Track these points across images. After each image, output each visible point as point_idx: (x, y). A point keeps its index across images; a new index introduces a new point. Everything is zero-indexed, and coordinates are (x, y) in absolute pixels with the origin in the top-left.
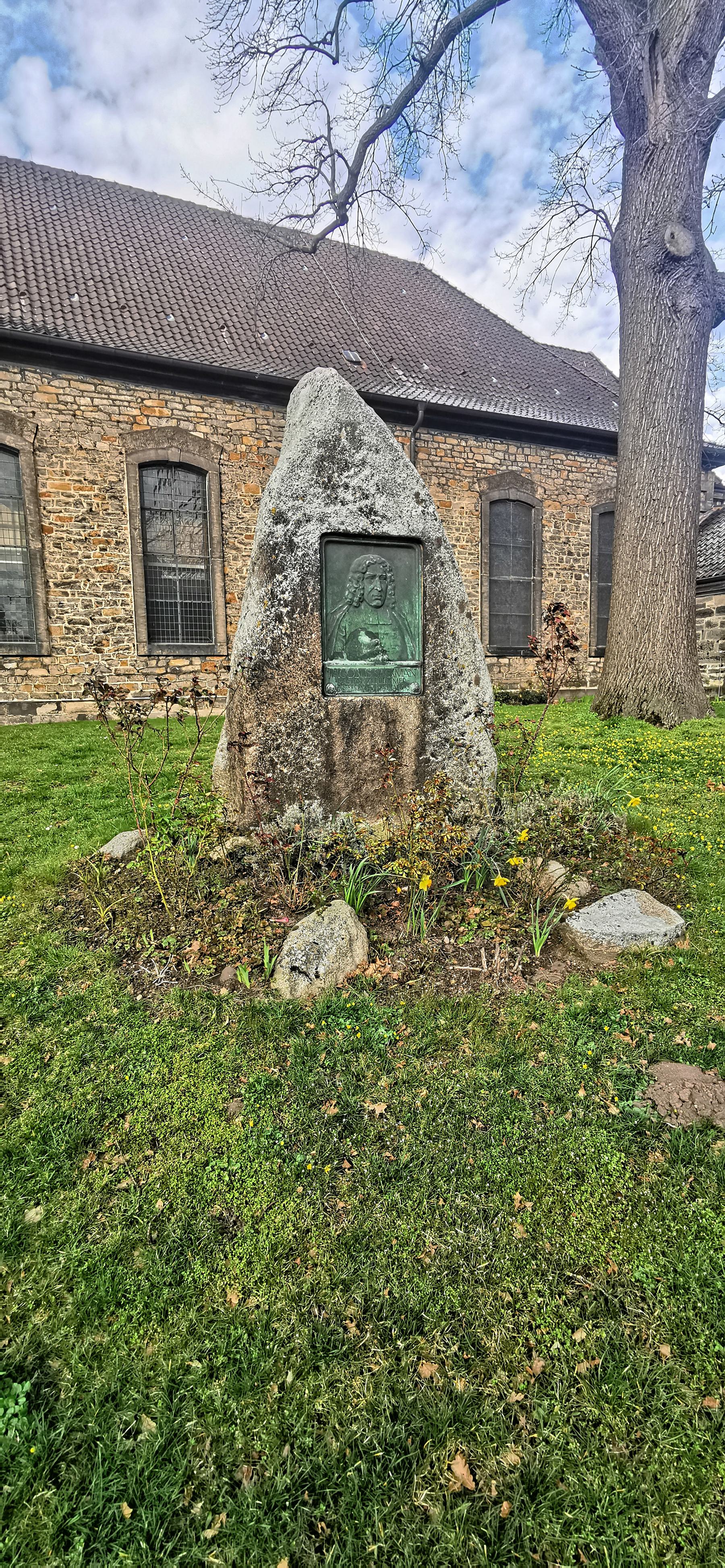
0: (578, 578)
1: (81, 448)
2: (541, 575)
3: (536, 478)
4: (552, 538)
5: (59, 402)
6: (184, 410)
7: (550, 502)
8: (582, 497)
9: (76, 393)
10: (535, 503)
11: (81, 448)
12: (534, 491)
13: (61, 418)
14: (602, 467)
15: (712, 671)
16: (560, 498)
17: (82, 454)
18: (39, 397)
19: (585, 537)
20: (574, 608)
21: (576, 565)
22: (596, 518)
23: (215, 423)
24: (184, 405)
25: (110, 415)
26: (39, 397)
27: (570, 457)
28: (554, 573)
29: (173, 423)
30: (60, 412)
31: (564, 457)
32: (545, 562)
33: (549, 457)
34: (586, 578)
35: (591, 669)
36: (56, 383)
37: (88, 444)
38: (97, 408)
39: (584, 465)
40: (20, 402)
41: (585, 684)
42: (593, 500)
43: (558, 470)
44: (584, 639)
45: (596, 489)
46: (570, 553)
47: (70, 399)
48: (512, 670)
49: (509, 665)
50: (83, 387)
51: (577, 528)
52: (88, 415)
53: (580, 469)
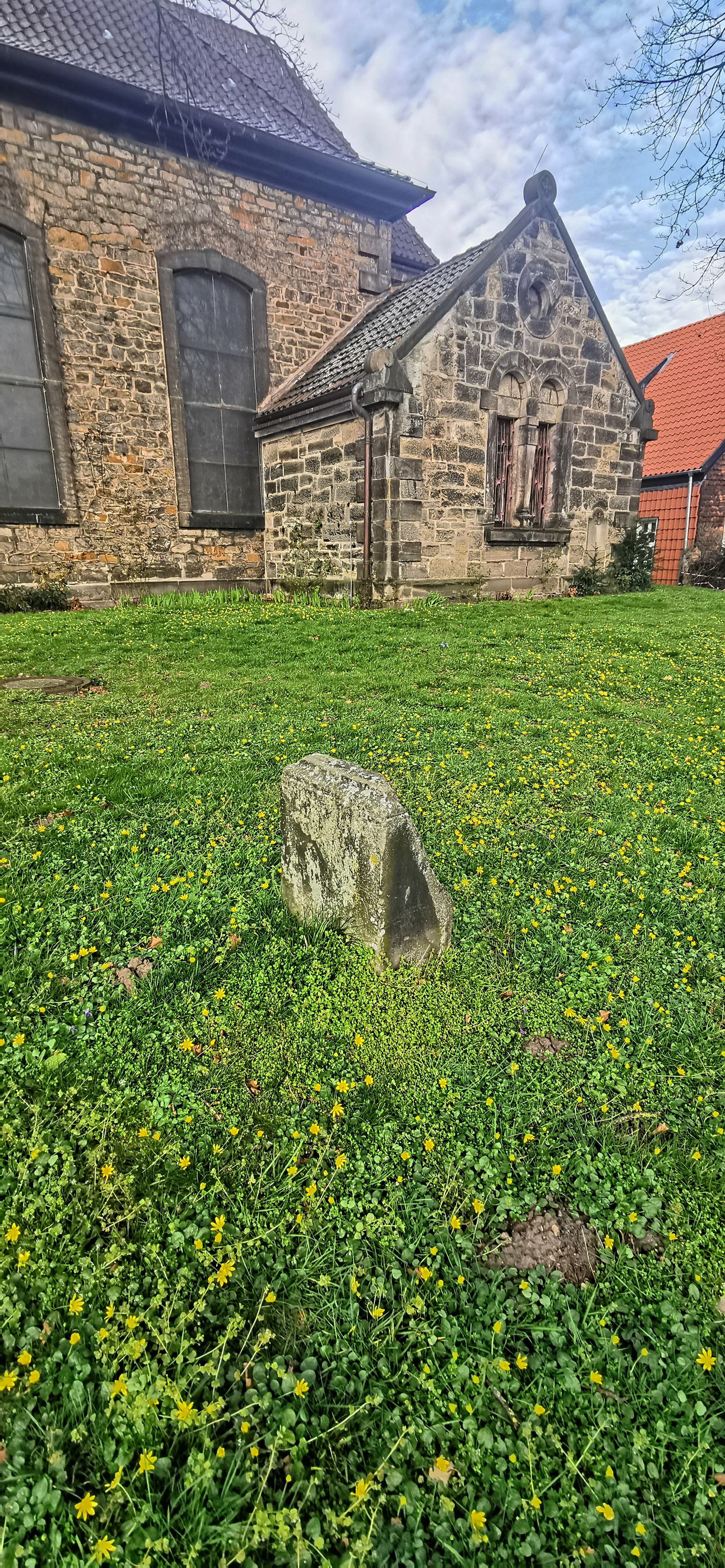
0: (144, 388)
2: (61, 375)
3: (22, 176)
4: (76, 305)
7: (63, 233)
8: (134, 232)
10: (24, 228)
12: (21, 205)
14: (170, 177)
15: (347, 555)
16: (84, 226)
19: (149, 312)
20: (140, 442)
21: (137, 364)
22: (166, 277)
27: (96, 145)
28: (91, 374)
31: (83, 144)
32: (67, 350)
33: (47, 138)
34: (159, 389)
35: (186, 548)
39: (131, 167)
41: (177, 572)
42: (159, 242)
43: (72, 168)
44: (168, 498)
45: (161, 219)
46: (120, 340)
48: (22, 549)
49: (15, 540)
51: (130, 292)
53: (123, 175)
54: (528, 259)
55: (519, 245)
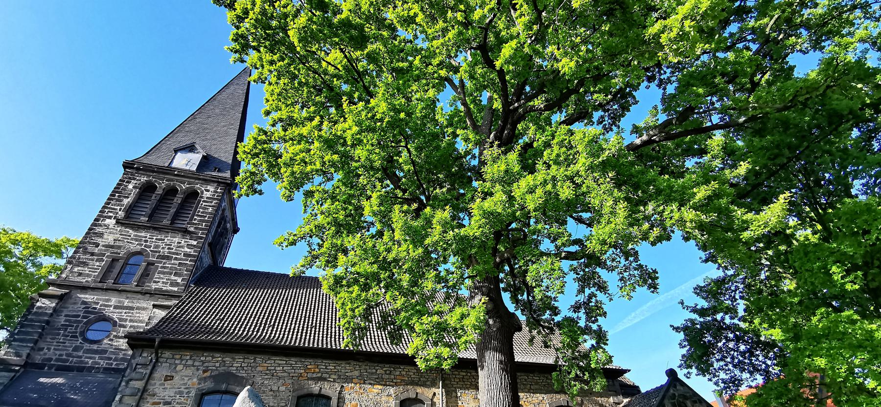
1: (271, 390)
5: (267, 370)
6: (326, 368)
9: (277, 365)
11: (271, 390)
13: (266, 377)
17: (271, 393)
18: (259, 369)
23: (340, 373)
24: (326, 366)
25: (289, 373)
26: (259, 369)
29: (319, 375)
30: (267, 374)
36: (269, 362)
37: (275, 388)
38: (284, 371)
40: (250, 372)
47: (273, 368)
50: (280, 362)
52: (279, 374)
54: (677, 395)
55: (672, 391)
